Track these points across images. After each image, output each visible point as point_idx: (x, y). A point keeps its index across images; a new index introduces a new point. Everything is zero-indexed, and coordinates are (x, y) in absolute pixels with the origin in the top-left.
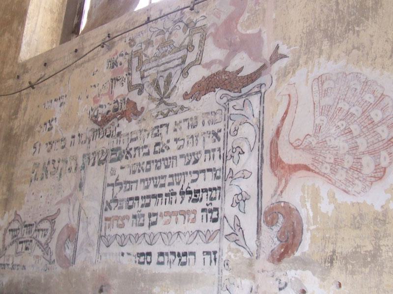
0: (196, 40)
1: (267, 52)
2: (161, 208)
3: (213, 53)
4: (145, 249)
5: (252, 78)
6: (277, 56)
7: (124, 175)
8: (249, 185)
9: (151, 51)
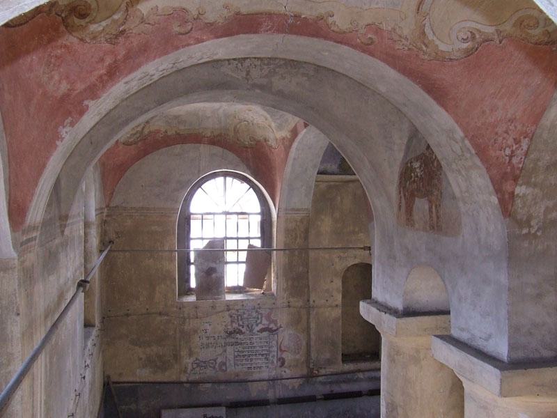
0: (260, 317)
1: (279, 325)
3: (265, 322)
5: (275, 330)
7: (241, 349)
8: (276, 354)
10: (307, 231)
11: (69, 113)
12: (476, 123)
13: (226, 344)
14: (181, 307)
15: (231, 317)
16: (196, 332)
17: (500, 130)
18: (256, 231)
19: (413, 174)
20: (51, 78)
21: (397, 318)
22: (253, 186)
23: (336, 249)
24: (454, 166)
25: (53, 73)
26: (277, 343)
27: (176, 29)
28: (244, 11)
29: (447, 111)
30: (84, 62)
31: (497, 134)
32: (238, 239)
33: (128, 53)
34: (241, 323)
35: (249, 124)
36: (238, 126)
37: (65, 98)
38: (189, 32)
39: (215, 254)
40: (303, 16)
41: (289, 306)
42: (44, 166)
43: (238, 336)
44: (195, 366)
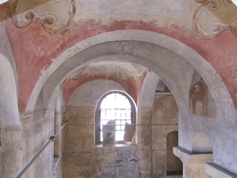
0: (130, 154)
1: (139, 158)
2: (128, 172)
3: (133, 156)
4: (126, 176)
5: (138, 160)
6: (139, 159)
7: (122, 169)
9: (124, 154)
10: (151, 117)
11: (45, 64)
12: (221, 67)
13: (116, 166)
14: (97, 149)
15: (118, 154)
16: (102, 160)
17: (232, 70)
18: (129, 117)
19: (195, 91)
20: (37, 49)
21: (189, 155)
22: (127, 97)
23: (164, 124)
24: (212, 86)
25: (38, 47)
26: (138, 166)
27: (90, 28)
28: (118, 20)
29: (208, 62)
30: (51, 43)
31: (231, 71)
32: (121, 120)
33: (69, 39)
34: (122, 157)
35: (125, 71)
36: (121, 72)
37: (42, 58)
38: (95, 29)
39: (111, 127)
40: (144, 22)
41: (143, 150)
42: (34, 86)
43: (121, 162)
44: (102, 176)
